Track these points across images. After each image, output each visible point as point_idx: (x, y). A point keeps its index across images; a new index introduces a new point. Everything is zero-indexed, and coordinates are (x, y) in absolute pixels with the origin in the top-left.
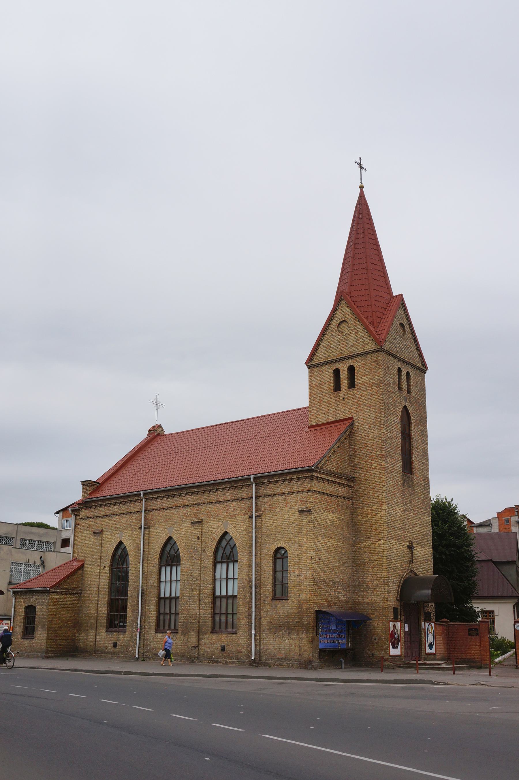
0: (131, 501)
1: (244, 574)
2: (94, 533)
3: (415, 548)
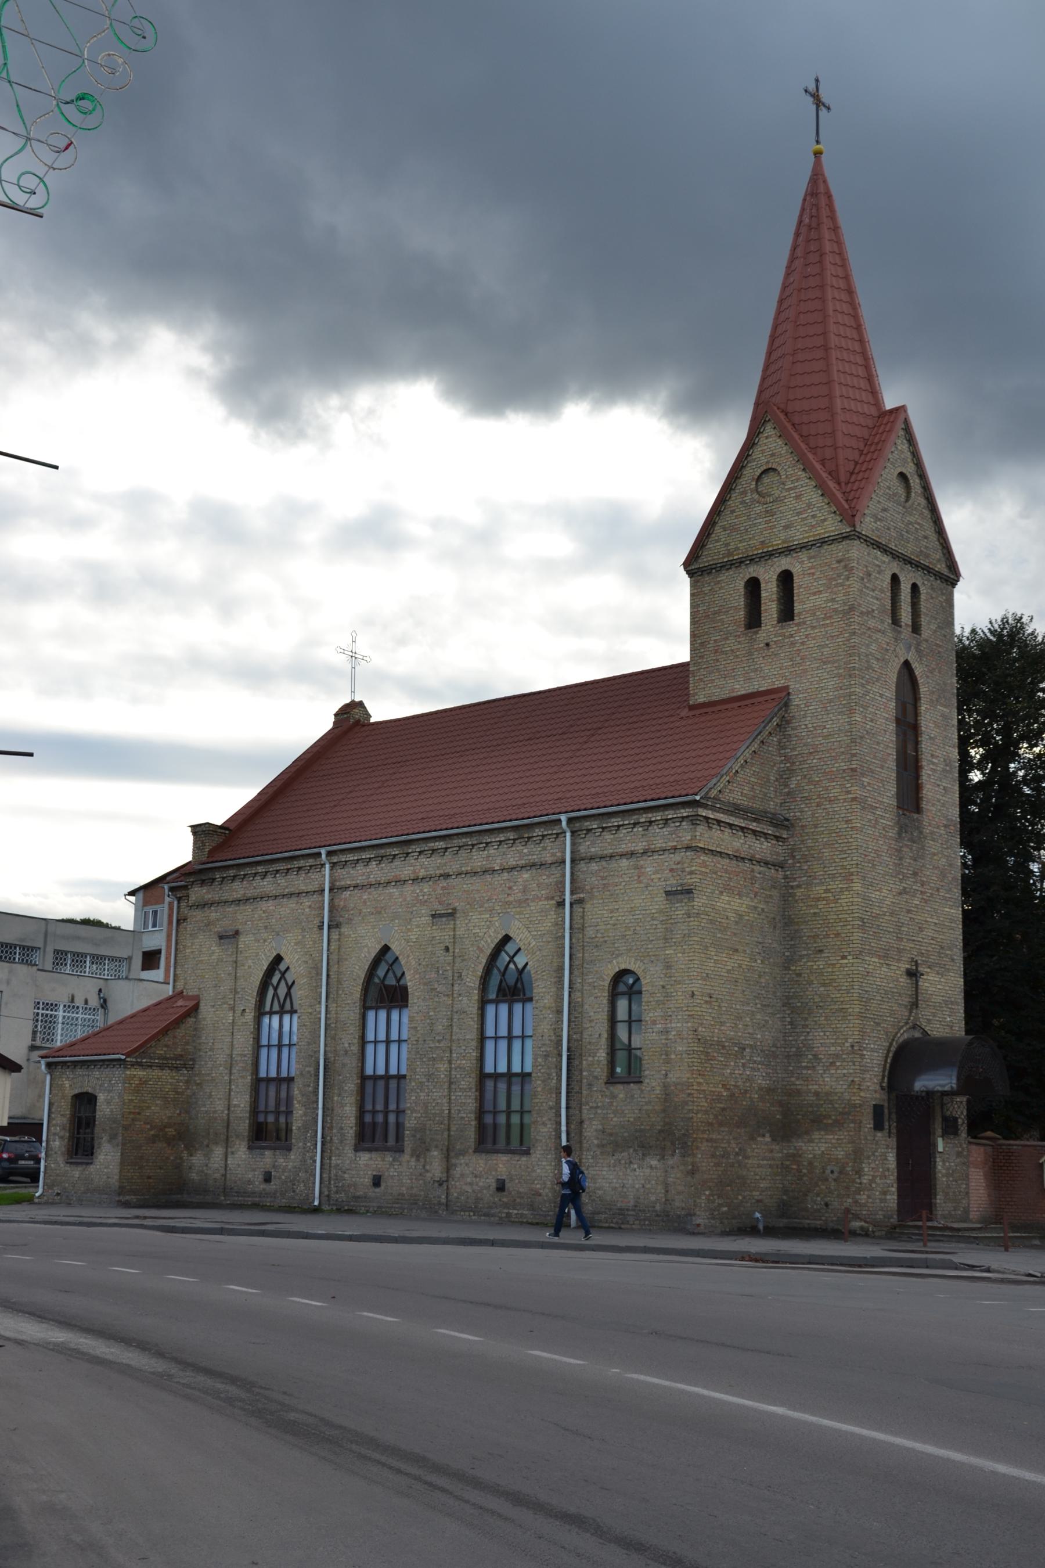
0: (299, 868)
1: (545, 1028)
3: (923, 975)
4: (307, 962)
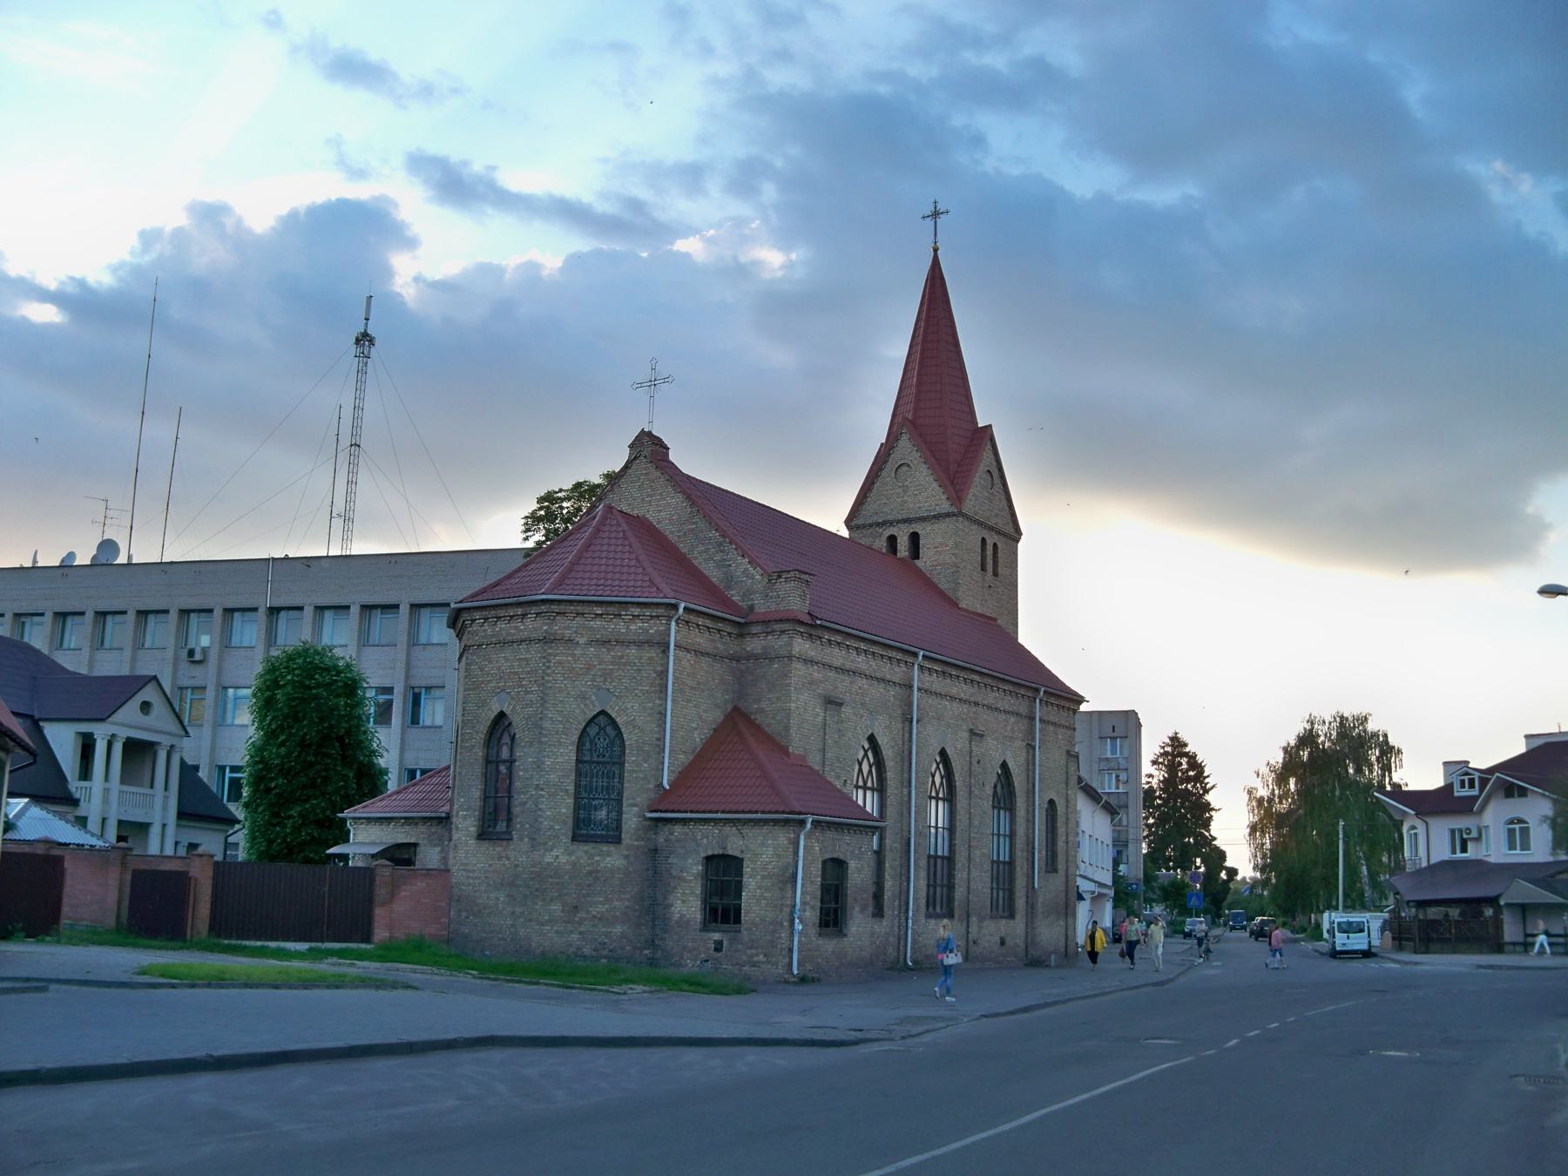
4: (893, 747)
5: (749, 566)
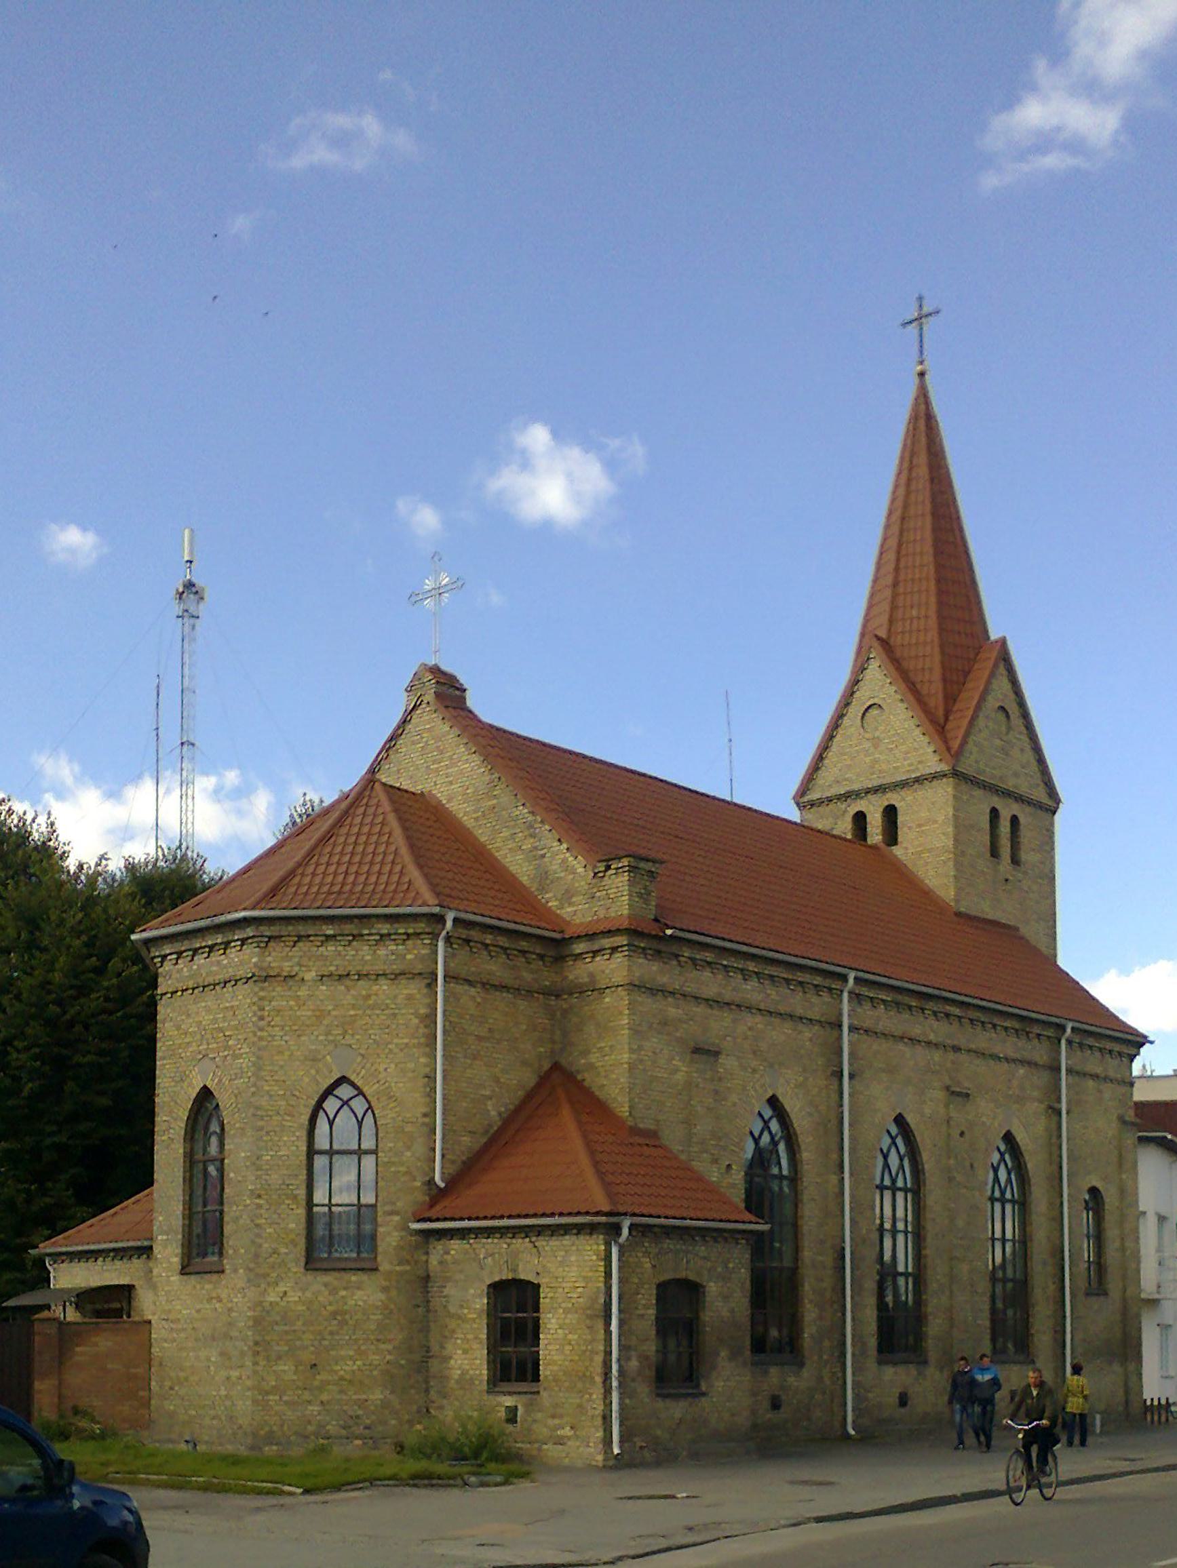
0: (801, 983)
2: (697, 1050)
5: (568, 855)
